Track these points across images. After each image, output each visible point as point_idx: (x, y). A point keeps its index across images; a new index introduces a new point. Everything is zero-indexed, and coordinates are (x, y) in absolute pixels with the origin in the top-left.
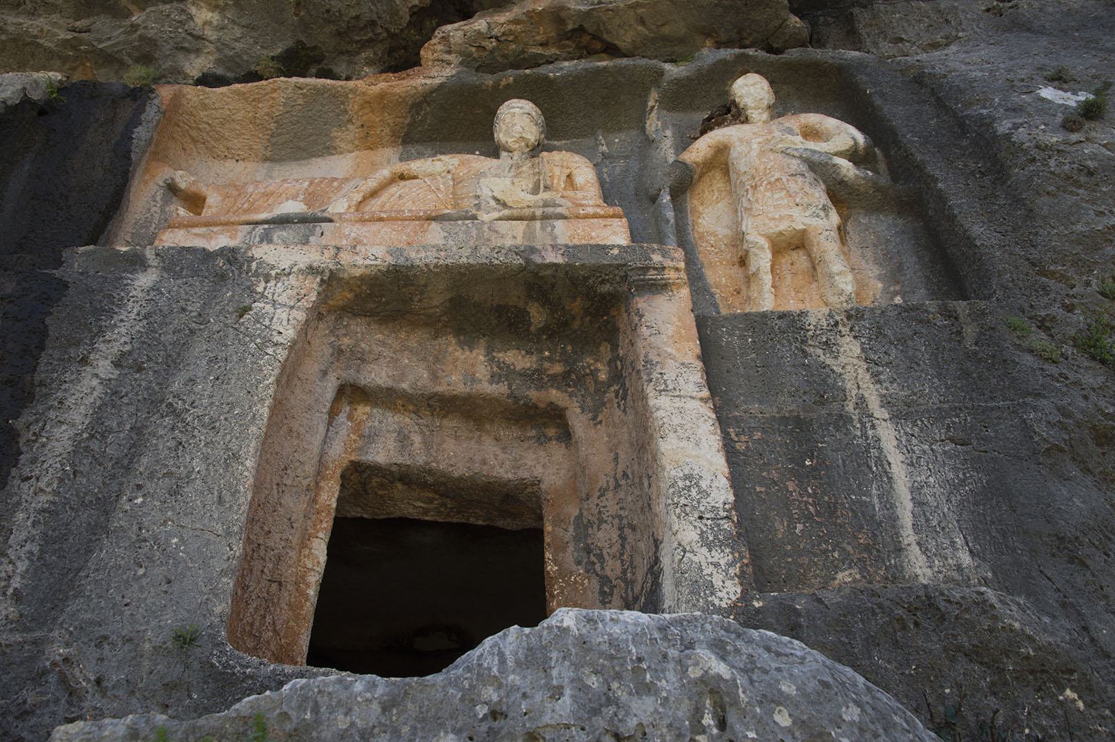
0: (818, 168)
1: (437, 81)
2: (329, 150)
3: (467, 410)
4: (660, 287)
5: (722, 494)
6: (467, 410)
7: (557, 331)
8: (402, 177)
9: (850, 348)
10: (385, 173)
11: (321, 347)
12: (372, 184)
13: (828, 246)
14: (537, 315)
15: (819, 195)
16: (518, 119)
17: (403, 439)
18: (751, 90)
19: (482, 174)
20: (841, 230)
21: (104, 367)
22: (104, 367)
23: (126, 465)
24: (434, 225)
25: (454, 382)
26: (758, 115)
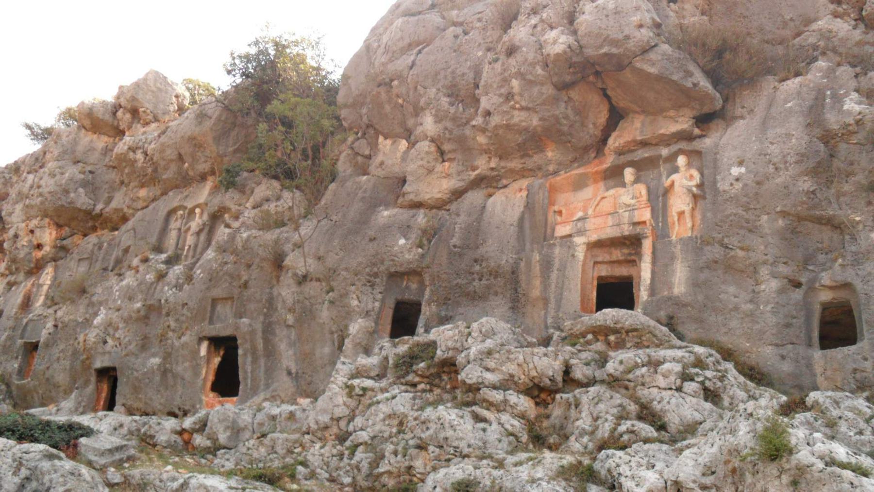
0: (689, 191)
1: (609, 165)
2: (587, 186)
3: (619, 262)
4: (646, 237)
5: (648, 282)
6: (619, 262)
7: (632, 244)
8: (603, 198)
9: (679, 247)
10: (599, 198)
11: (589, 256)
12: (596, 203)
13: (687, 215)
14: (628, 242)
15: (688, 199)
16: (629, 174)
17: (607, 271)
18: (681, 160)
19: (620, 196)
20: (693, 209)
21: (556, 272)
22: (556, 272)
23: (562, 288)
24: (610, 217)
25: (614, 258)
26: (682, 169)
